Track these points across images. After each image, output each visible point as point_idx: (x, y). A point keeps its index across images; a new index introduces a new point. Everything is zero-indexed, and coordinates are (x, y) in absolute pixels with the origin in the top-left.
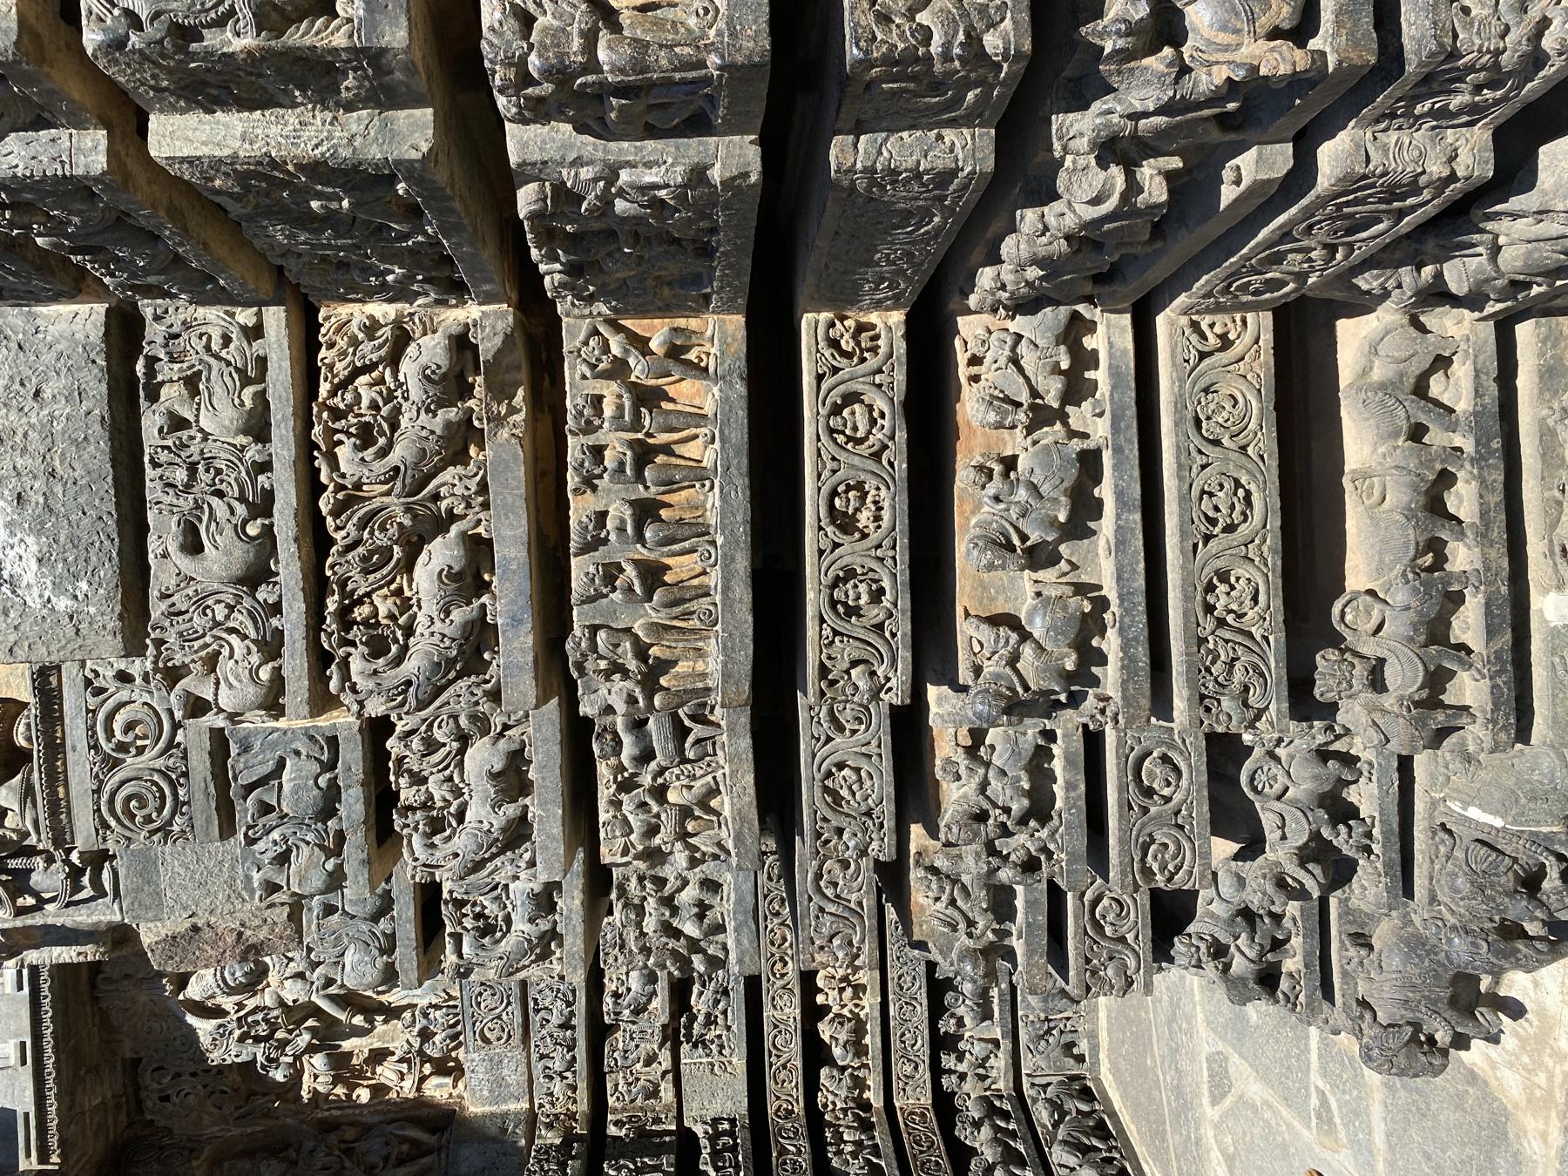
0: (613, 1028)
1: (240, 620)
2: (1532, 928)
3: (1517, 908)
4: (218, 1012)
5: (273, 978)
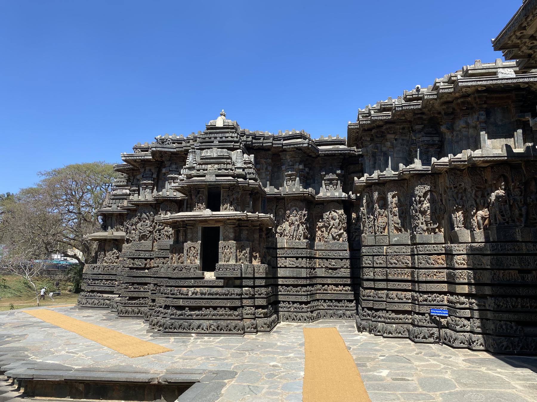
0: (327, 261)
3: (374, 326)
4: (329, 214)
5: (333, 221)
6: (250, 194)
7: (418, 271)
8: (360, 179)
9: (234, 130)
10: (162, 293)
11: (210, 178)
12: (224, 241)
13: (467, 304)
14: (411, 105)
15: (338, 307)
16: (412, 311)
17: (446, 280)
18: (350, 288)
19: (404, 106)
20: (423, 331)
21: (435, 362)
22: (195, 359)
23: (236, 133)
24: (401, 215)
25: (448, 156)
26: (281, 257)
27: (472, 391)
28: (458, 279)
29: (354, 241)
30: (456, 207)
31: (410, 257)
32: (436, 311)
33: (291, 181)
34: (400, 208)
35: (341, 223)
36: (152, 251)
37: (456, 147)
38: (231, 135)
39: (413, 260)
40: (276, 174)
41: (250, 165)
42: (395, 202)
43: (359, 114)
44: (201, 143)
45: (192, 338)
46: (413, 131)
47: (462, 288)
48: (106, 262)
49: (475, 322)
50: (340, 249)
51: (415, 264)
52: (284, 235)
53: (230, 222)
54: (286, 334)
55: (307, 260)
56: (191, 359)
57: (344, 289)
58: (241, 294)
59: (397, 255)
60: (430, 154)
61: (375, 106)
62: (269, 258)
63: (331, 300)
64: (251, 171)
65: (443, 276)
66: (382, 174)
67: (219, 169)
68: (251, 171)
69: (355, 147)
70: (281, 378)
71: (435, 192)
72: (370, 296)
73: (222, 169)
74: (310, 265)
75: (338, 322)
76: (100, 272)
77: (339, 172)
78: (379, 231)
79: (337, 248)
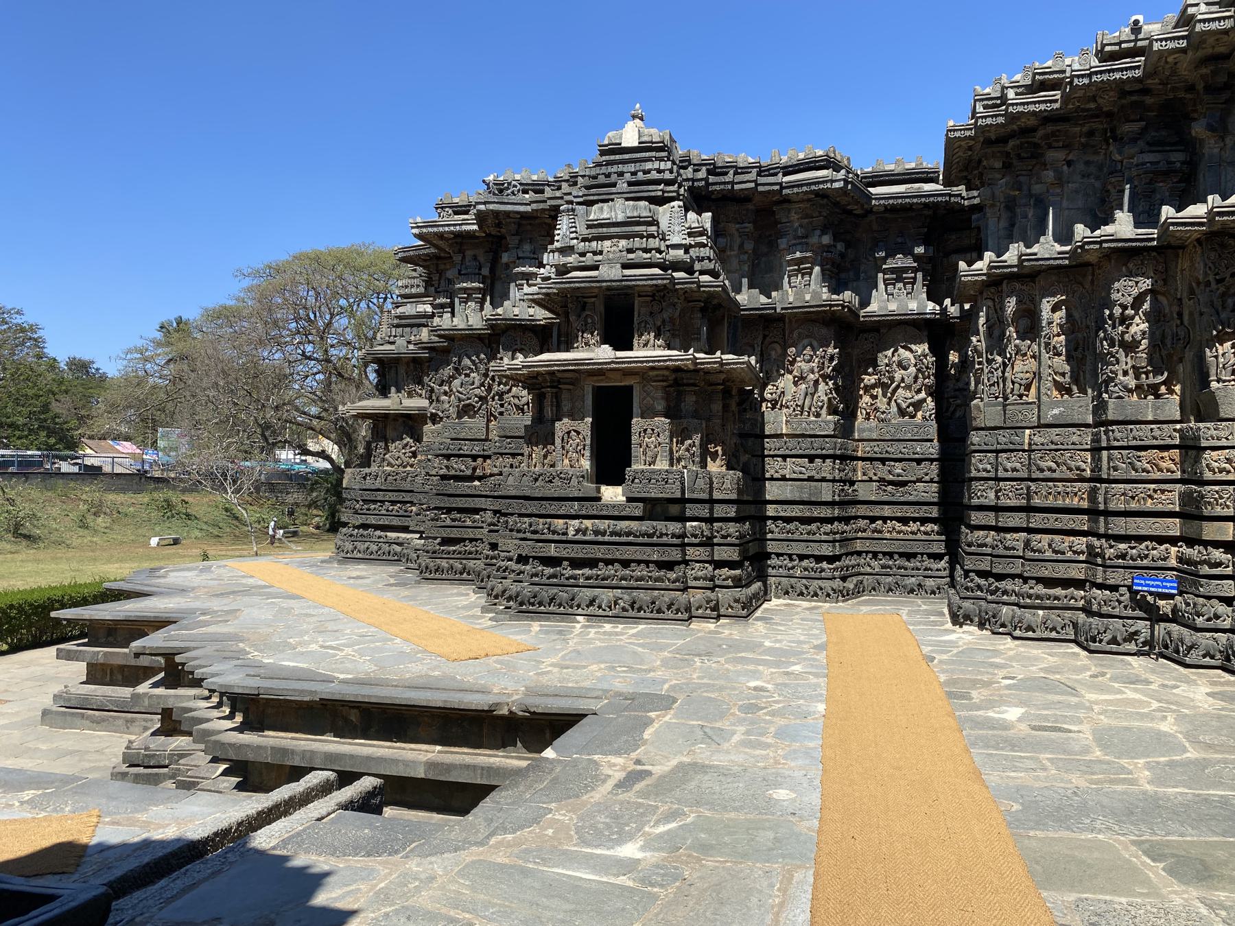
0: (884, 465)
3: (991, 613)
4: (893, 355)
5: (902, 372)
6: (703, 310)
7: (1106, 488)
8: (974, 267)
9: (664, 154)
10: (511, 530)
11: (610, 272)
12: (642, 417)
13: (1228, 567)
14: (1113, 71)
16: (1088, 581)
17: (1177, 509)
18: (936, 528)
19: (1096, 73)
20: (1111, 627)
21: (1137, 696)
22: (585, 667)
23: (669, 160)
24: (1073, 353)
25: (1205, 201)
26: (773, 456)
27: (1225, 761)
28: (1209, 508)
29: (951, 418)
30: (1219, 332)
31: (1088, 455)
32: (1148, 582)
33: (800, 276)
34: (1070, 337)
35: (920, 375)
36: (486, 440)
37: (1229, 177)
38: (656, 165)
39: (1097, 460)
40: (763, 259)
41: (703, 239)
43: (975, 101)
44: (587, 188)
45: (578, 626)
46: (1115, 140)
47: (1220, 528)
48: (389, 464)
51: (1100, 470)
52: (782, 405)
53: (657, 376)
54: (784, 625)
55: (834, 463)
56: (577, 667)
57: (922, 529)
58: (683, 536)
59: (1057, 450)
60: (1158, 196)
61: (1018, 77)
62: (745, 458)
63: (890, 555)
64: (705, 252)
65: (1171, 499)
66: (1028, 251)
67: (630, 251)
68: (705, 252)
69: (963, 187)
70: (773, 714)
71: (1163, 294)
72: (986, 546)
73: (637, 249)
74: (842, 474)
75: (906, 602)
76: (377, 485)
77: (920, 250)
79: (909, 436)
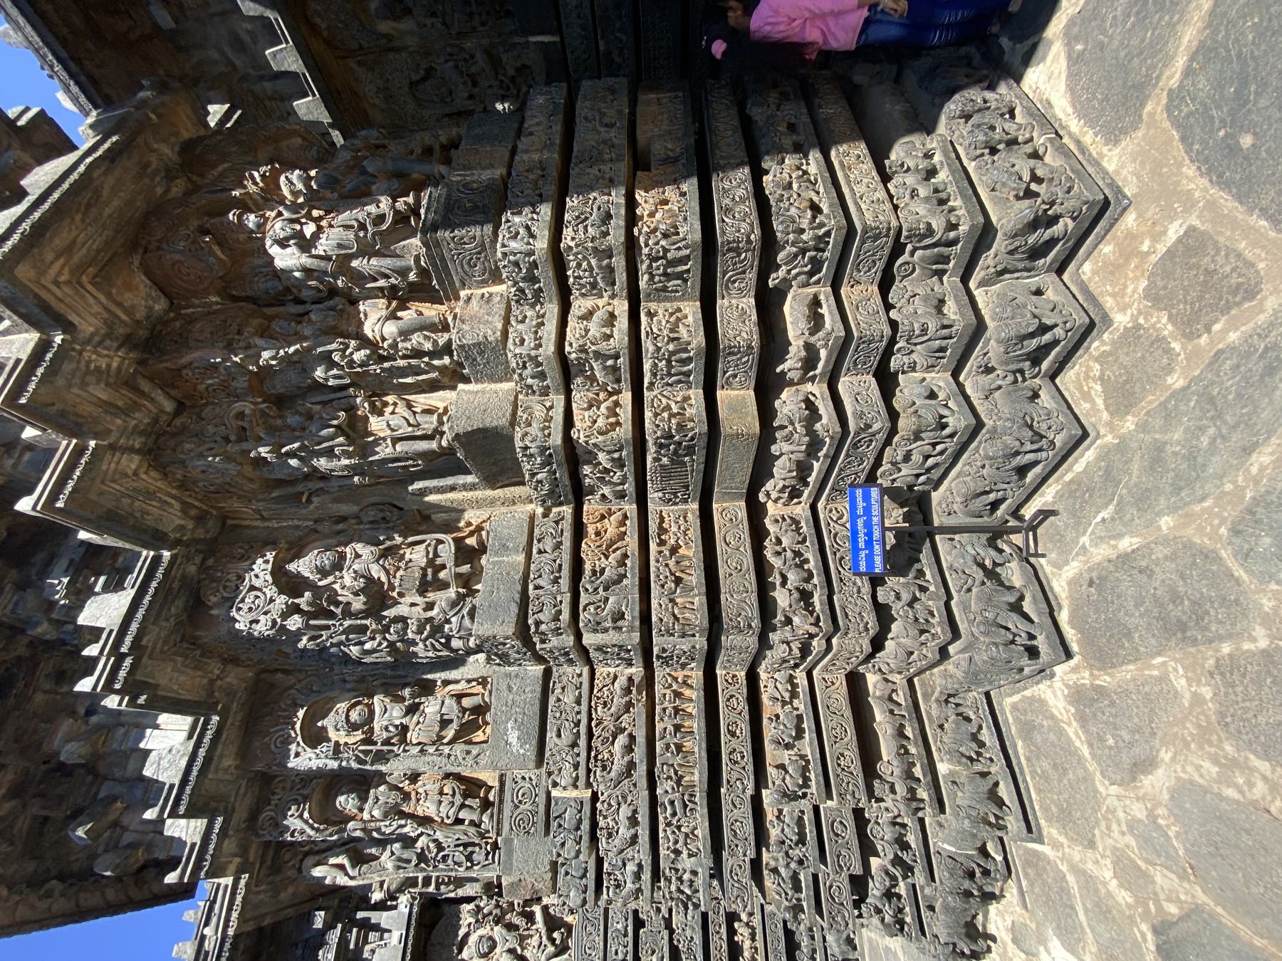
1: (569, 758)
2: (976, 893)
3: (967, 884)
5: (498, 950)
15: (814, 951)
17: (695, 506)
32: (862, 545)
42: (342, 733)
49: (916, 326)
50: (602, 928)
59: (590, 735)
77: (319, 919)
78: (475, 817)
